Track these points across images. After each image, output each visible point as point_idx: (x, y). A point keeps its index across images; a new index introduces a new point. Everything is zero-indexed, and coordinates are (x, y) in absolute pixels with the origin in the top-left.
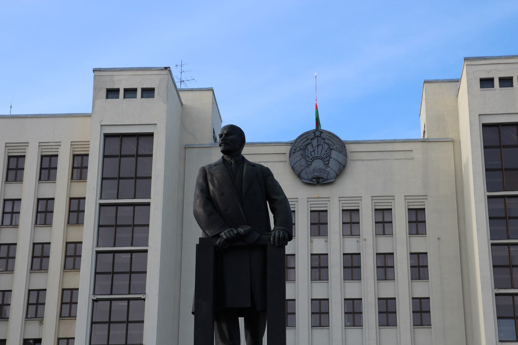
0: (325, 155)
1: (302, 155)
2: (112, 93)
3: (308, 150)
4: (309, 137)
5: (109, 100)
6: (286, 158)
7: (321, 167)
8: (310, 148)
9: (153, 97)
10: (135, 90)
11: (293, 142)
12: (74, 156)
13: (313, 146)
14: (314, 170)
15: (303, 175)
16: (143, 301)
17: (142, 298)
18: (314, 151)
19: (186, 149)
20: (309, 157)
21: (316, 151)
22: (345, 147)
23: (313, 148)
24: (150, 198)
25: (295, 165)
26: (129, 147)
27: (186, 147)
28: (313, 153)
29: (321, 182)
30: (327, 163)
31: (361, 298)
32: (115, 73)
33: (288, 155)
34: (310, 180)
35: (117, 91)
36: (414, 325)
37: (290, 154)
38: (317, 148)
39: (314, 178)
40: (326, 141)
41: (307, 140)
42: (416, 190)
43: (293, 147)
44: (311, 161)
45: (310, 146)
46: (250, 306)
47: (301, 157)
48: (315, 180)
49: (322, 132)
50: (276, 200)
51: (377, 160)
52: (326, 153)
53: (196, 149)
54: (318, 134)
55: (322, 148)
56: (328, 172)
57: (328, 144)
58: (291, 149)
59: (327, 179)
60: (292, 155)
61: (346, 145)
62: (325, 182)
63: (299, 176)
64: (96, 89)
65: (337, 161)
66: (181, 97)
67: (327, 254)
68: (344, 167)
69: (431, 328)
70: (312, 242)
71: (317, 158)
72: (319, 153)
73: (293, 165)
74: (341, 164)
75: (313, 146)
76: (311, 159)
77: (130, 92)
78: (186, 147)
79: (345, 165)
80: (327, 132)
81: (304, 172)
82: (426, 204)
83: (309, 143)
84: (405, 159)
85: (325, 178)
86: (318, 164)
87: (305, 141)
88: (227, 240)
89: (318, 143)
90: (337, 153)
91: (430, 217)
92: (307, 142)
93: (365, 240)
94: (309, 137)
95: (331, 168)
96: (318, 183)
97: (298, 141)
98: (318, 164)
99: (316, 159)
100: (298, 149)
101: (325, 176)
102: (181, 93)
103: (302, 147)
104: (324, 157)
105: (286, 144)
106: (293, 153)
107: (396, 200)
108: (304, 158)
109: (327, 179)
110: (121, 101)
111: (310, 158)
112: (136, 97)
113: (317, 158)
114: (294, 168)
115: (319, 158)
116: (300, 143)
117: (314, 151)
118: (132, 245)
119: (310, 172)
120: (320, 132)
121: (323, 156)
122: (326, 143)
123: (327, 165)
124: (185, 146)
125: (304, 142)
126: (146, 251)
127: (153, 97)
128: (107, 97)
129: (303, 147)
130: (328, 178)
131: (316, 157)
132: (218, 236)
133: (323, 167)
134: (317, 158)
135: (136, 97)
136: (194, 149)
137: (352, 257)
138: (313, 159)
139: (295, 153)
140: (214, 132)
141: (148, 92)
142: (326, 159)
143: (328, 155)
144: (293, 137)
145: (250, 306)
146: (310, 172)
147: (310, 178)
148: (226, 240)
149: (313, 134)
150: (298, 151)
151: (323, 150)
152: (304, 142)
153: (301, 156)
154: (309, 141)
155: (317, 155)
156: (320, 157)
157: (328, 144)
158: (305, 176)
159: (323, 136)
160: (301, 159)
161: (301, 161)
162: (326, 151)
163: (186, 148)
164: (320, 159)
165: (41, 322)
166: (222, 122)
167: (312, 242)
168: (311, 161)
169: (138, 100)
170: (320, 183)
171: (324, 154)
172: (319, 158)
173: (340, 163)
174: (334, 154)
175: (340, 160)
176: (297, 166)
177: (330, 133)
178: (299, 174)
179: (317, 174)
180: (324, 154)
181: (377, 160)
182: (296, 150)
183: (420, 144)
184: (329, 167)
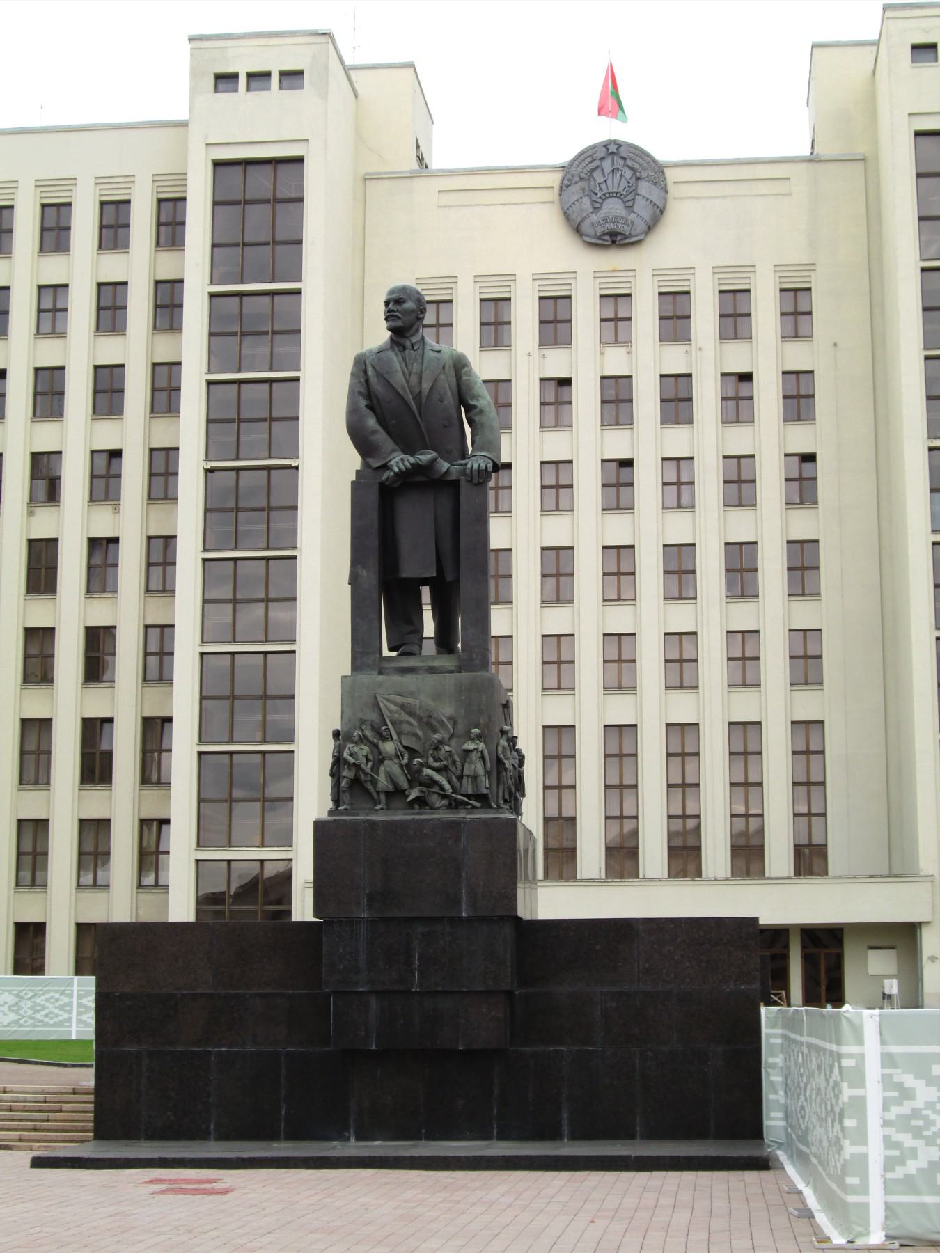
0: (627, 189)
1: (583, 189)
2: (225, 80)
3: (595, 180)
5: (220, 95)
6: (553, 195)
7: (619, 211)
8: (598, 176)
9: (302, 88)
10: (267, 75)
11: (566, 165)
12: (160, 201)
13: (603, 173)
14: (606, 219)
15: (586, 227)
16: (294, 470)
18: (606, 181)
19: (367, 181)
20: (596, 194)
21: (609, 182)
22: (663, 173)
23: (604, 177)
24: (299, 279)
25: (570, 209)
26: (260, 182)
27: (367, 178)
28: (603, 186)
29: (620, 240)
30: (630, 204)
31: (692, 455)
32: (230, 43)
33: (557, 189)
34: (599, 238)
35: (234, 77)
36: (787, 504)
37: (561, 187)
38: (611, 175)
39: (605, 234)
40: (629, 163)
41: (592, 161)
42: (795, 253)
43: (565, 176)
44: (600, 200)
46: (434, 575)
47: (582, 195)
48: (607, 238)
49: (620, 146)
50: (474, 407)
51: (724, 197)
52: (629, 186)
53: (386, 182)
54: (613, 148)
55: (622, 175)
56: (633, 223)
57: (632, 169)
58: (563, 180)
59: (630, 236)
60: (565, 190)
61: (667, 171)
62: (627, 241)
63: (577, 230)
64: (195, 74)
65: (649, 202)
66: (354, 81)
67: (630, 377)
68: (662, 212)
69: (817, 508)
70: (602, 354)
71: (611, 195)
72: (616, 186)
73: (565, 209)
74: (656, 207)
75: (603, 173)
76: (600, 197)
77: (258, 78)
78: (367, 177)
79: (664, 208)
80: (630, 145)
81: (587, 222)
82: (813, 279)
83: (597, 167)
84: (776, 194)
85: (627, 234)
86: (613, 207)
88: (400, 475)
89: (613, 165)
90: (650, 184)
91: (820, 304)
92: (592, 165)
93: (700, 349)
94: (595, 155)
95: (638, 215)
96: (614, 242)
97: (576, 162)
99: (610, 197)
101: (626, 230)
102: (353, 74)
103: (583, 175)
104: (624, 193)
105: (554, 169)
106: (567, 187)
107: (757, 274)
108: (587, 195)
109: (630, 236)
110: (242, 95)
111: (599, 196)
112: (268, 89)
113: (611, 195)
115: (615, 195)
116: (581, 166)
117: (606, 181)
118: (271, 369)
119: (599, 222)
120: (618, 144)
121: (624, 190)
122: (628, 166)
123: (630, 208)
124: (364, 176)
125: (587, 165)
126: (297, 380)
127: (302, 88)
128: (216, 90)
129: (586, 174)
130: (633, 232)
131: (609, 193)
132: (385, 467)
134: (612, 195)
135: (268, 89)
136: (380, 181)
137: (676, 381)
138: (603, 197)
139: (570, 185)
140: (418, 147)
141: (292, 77)
142: (628, 198)
143: (633, 189)
144: (565, 153)
145: (434, 575)
146: (599, 222)
147: (599, 234)
148: (396, 474)
149: (604, 149)
150: (576, 183)
151: (623, 179)
153: (581, 191)
155: (611, 190)
156: (617, 193)
157: (632, 169)
158: (590, 231)
159: (623, 152)
160: (581, 198)
161: (582, 202)
162: (629, 182)
163: (365, 179)
164: (616, 197)
165: (117, 510)
166: (433, 123)
167: (602, 354)
168: (600, 200)
170: (617, 243)
171: (625, 188)
172: (615, 195)
173: (655, 204)
174: (644, 188)
175: (654, 198)
176: (573, 211)
177: (635, 147)
178: (578, 226)
179: (611, 227)
180: (625, 188)
181: (724, 197)
182: (572, 180)
183: (804, 166)
184: (634, 212)
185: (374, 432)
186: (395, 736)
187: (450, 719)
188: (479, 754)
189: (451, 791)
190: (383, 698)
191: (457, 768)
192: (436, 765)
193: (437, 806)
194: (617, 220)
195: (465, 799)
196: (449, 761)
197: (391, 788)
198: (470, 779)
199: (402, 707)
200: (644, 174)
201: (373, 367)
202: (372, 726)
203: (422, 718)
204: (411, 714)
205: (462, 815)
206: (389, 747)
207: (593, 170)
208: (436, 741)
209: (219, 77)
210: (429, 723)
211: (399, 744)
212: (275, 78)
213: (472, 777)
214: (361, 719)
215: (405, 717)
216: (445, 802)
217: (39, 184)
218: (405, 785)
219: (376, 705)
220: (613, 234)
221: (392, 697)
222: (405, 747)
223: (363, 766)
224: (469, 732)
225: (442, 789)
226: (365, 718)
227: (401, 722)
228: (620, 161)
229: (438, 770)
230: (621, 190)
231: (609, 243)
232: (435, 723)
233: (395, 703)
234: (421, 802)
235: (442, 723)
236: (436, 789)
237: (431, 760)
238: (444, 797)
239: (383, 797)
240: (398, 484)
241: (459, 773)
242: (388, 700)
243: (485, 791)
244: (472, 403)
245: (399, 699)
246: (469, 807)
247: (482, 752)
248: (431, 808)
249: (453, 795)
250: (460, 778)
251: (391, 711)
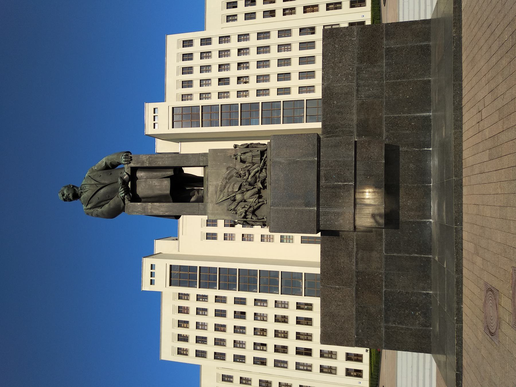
10: (151, 272)
35: (151, 280)
169: (156, 271)
185: (110, 205)
186: (234, 194)
187: (227, 169)
188: (243, 155)
189: (258, 168)
191: (249, 166)
193: (265, 175)
195: (262, 161)
196: (246, 169)
197: (257, 195)
199: (221, 191)
201: (87, 206)
203: (227, 182)
204: (225, 187)
206: (239, 197)
208: (236, 175)
209: (151, 284)
210: (229, 178)
211: (237, 192)
212: (152, 271)
213: (252, 158)
215: (226, 190)
216: (264, 170)
217: (173, 327)
218: (256, 190)
221: (217, 197)
222: (239, 190)
223: (246, 209)
225: (258, 171)
226: (226, 208)
227: (228, 192)
229: (250, 174)
232: (229, 176)
233: (220, 195)
234: (263, 183)
235: (229, 174)
236: (257, 174)
237: (245, 178)
238: (261, 170)
239: (260, 200)
240: (131, 194)
241: (251, 165)
243: (259, 152)
244: (104, 163)
245: (218, 194)
246: (266, 159)
248: (267, 177)
249: (260, 167)
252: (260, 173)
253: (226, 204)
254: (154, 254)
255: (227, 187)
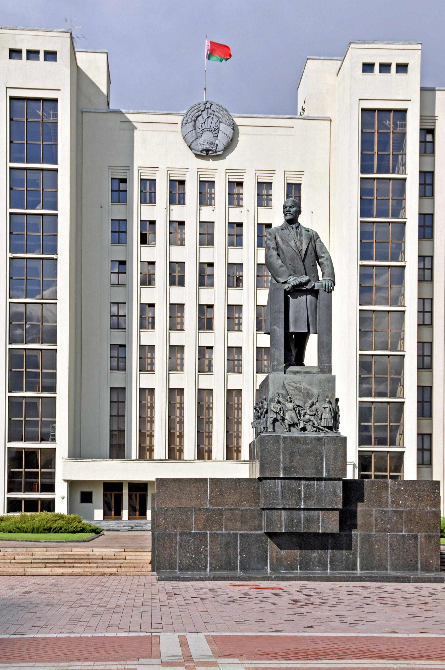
3: (199, 121)
4: (200, 109)
15: (193, 146)
17: (55, 258)
18: (204, 123)
28: (203, 125)
29: (210, 154)
30: (216, 135)
37: (182, 124)
40: (216, 113)
41: (198, 112)
45: (201, 117)
48: (205, 152)
57: (218, 117)
59: (216, 152)
65: (225, 134)
71: (207, 130)
75: (203, 118)
76: (202, 131)
81: (195, 143)
84: (287, 135)
86: (207, 136)
87: (197, 112)
94: (200, 109)
98: (207, 136)
100: (190, 120)
101: (214, 148)
106: (185, 124)
111: (201, 130)
114: (186, 139)
115: (209, 130)
117: (204, 123)
125: (196, 113)
133: (213, 139)
139: (187, 123)
147: (201, 150)
152: (196, 113)
154: (200, 113)
155: (207, 128)
157: (218, 117)
158: (197, 148)
160: (192, 130)
164: (209, 131)
172: (209, 130)
178: (190, 146)
179: (207, 146)
190: (287, 384)
192: (311, 413)
194: (210, 143)
195: (323, 428)
198: (325, 419)
199: (296, 388)
200: (224, 120)
202: (282, 396)
204: (299, 391)
205: (322, 434)
207: (198, 117)
210: (308, 395)
214: (277, 393)
215: (297, 392)
219: (284, 387)
220: (207, 151)
221: (291, 384)
222: (297, 406)
224: (325, 400)
225: (314, 424)
226: (280, 393)
228: (212, 113)
230: (212, 128)
231: (205, 154)
233: (293, 387)
241: (320, 417)
242: (289, 385)
245: (294, 385)
247: (330, 409)
250: (321, 419)
251: (291, 390)
252: (312, 426)
253: (284, 392)
254: (76, 50)
255: (299, 393)
